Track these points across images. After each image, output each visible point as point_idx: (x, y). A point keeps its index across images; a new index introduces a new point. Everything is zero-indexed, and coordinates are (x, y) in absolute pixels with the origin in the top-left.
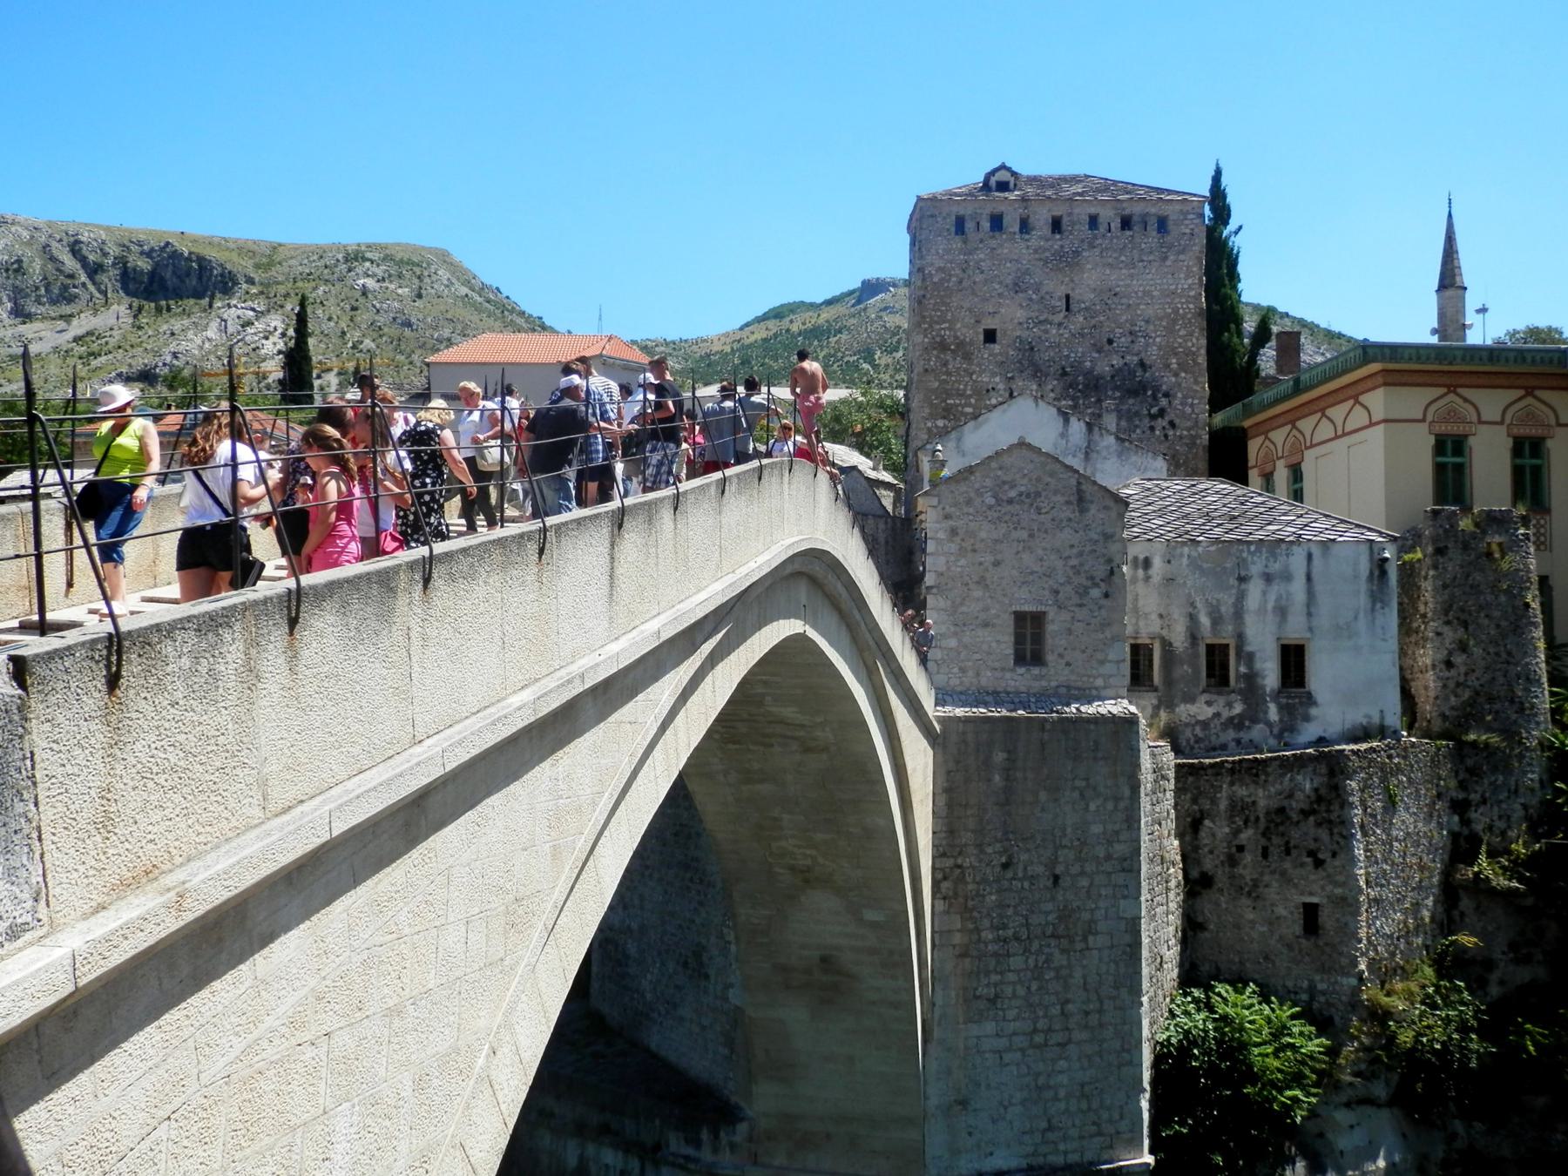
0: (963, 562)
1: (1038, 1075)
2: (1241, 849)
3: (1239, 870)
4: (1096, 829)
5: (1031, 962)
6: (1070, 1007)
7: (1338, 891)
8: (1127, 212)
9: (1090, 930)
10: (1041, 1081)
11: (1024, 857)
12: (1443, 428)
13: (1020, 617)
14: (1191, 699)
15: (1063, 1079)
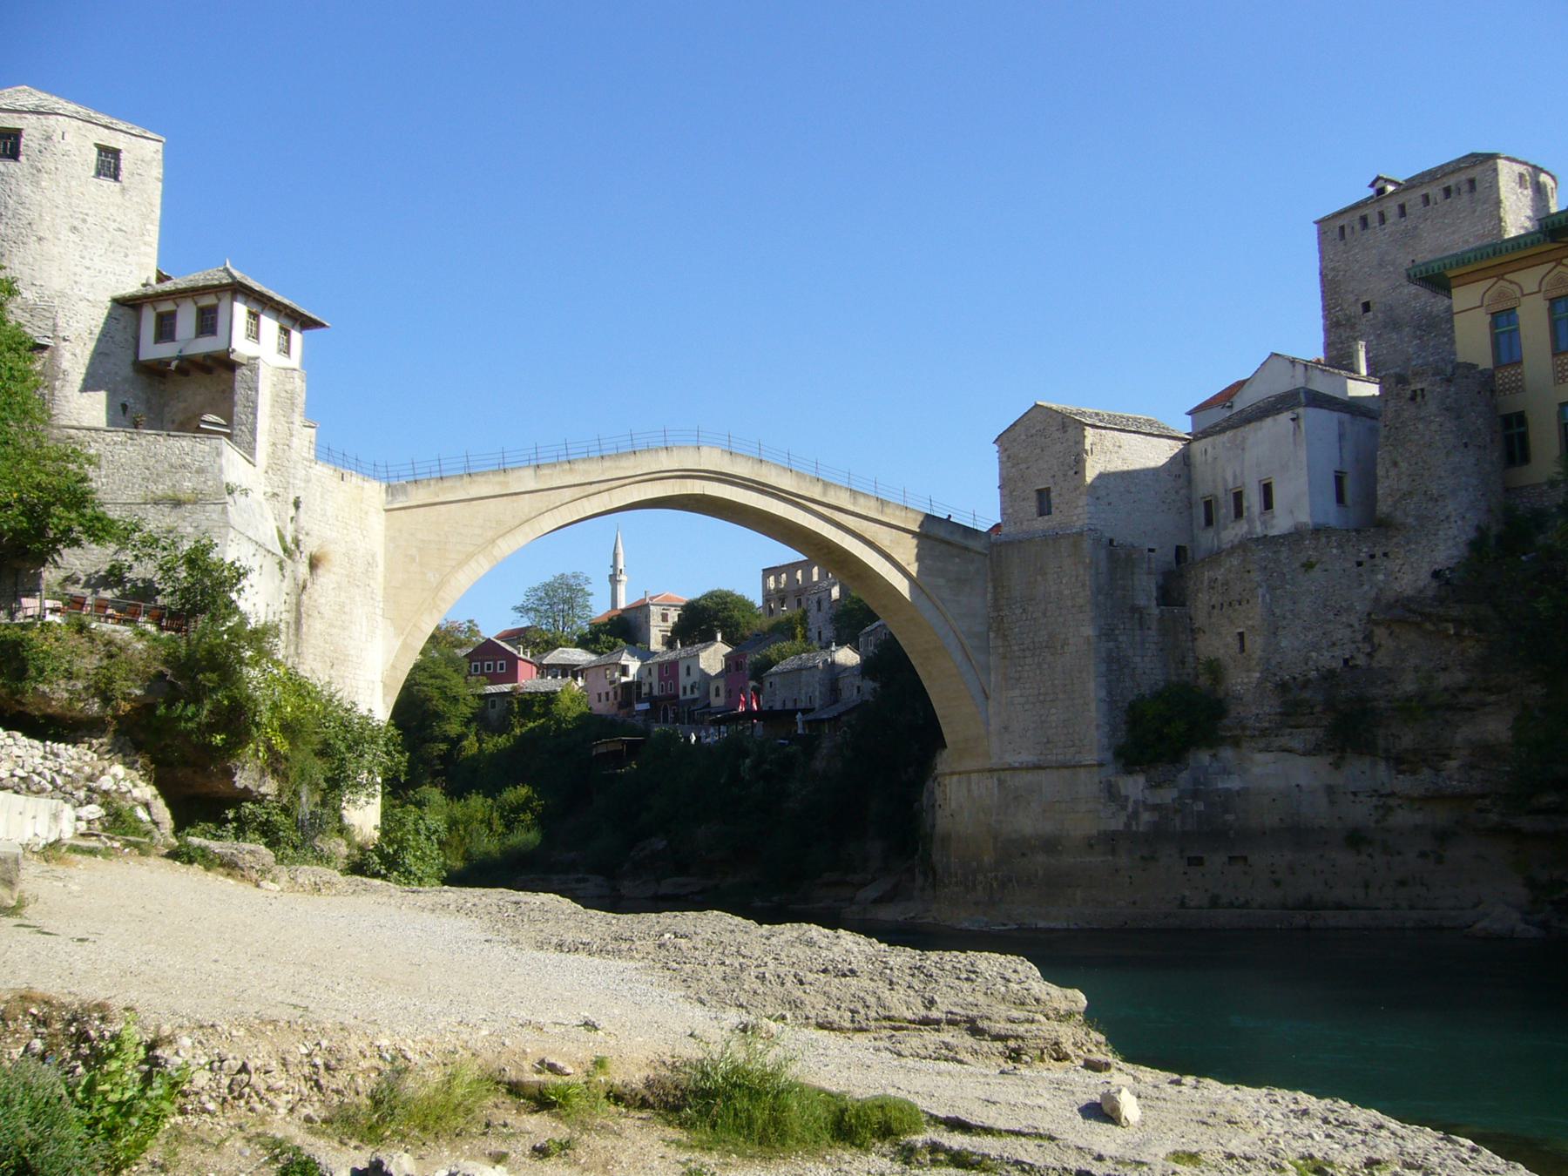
0: (1014, 470)
1: (1041, 715)
2: (1213, 607)
3: (1213, 620)
4: (1067, 592)
5: (1036, 660)
6: (1056, 682)
7: (1250, 623)
8: (1446, 185)
9: (1065, 643)
10: (1043, 718)
11: (1030, 609)
12: (1496, 308)
13: (1039, 492)
14: (1225, 528)
15: (1054, 718)
